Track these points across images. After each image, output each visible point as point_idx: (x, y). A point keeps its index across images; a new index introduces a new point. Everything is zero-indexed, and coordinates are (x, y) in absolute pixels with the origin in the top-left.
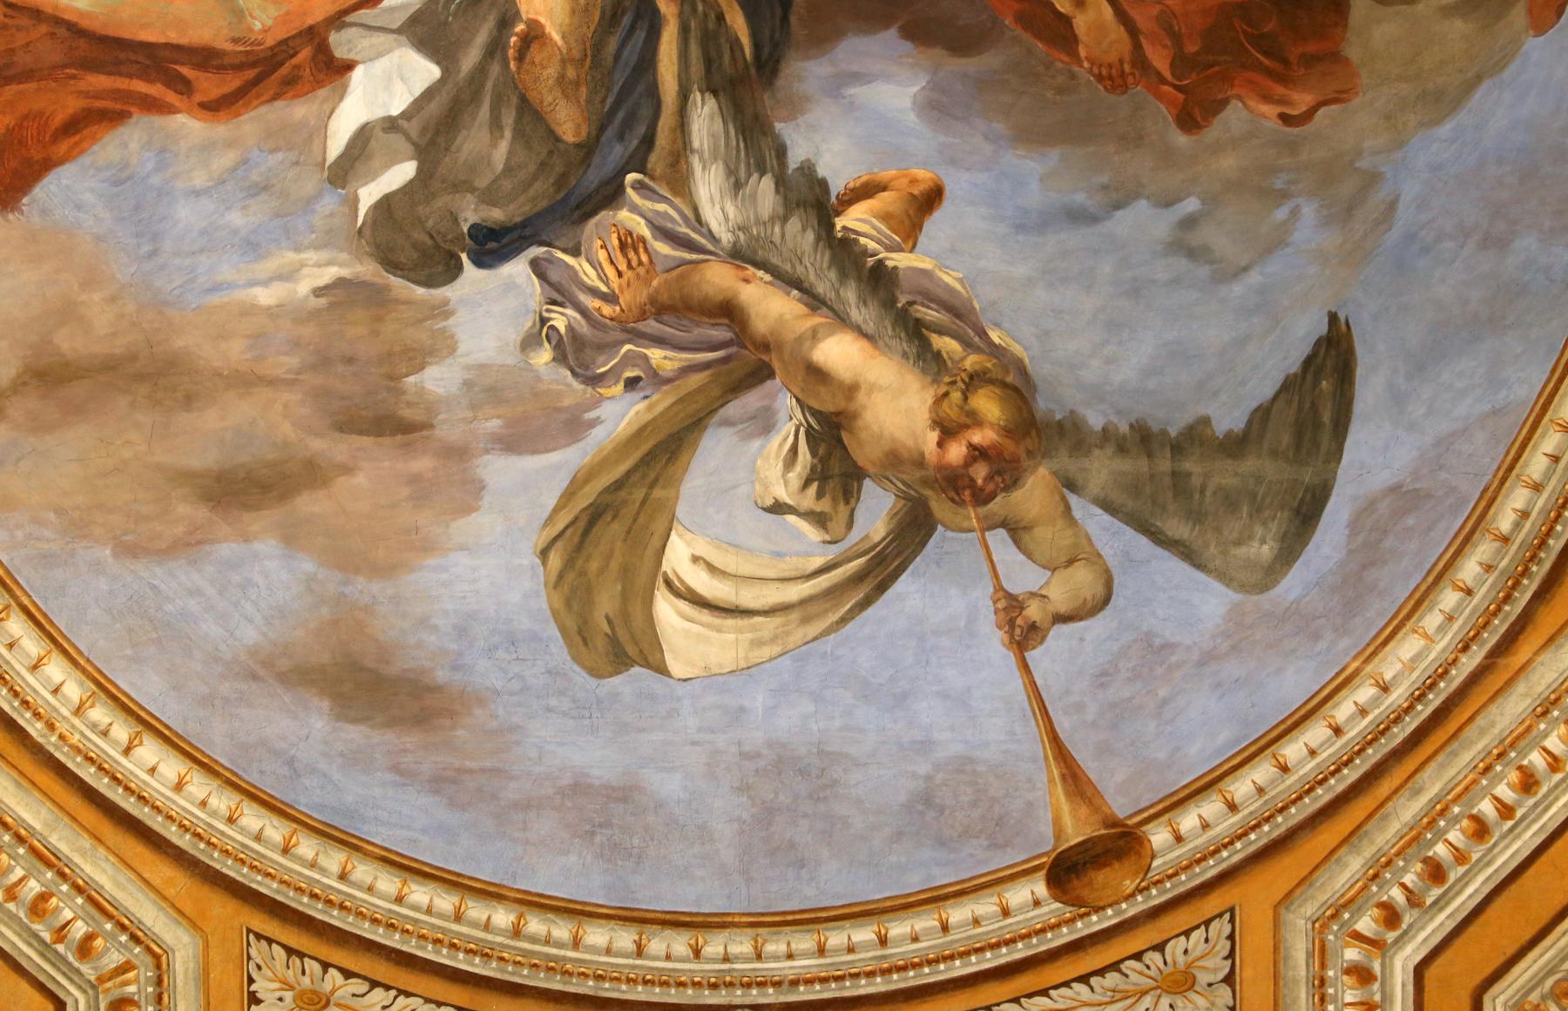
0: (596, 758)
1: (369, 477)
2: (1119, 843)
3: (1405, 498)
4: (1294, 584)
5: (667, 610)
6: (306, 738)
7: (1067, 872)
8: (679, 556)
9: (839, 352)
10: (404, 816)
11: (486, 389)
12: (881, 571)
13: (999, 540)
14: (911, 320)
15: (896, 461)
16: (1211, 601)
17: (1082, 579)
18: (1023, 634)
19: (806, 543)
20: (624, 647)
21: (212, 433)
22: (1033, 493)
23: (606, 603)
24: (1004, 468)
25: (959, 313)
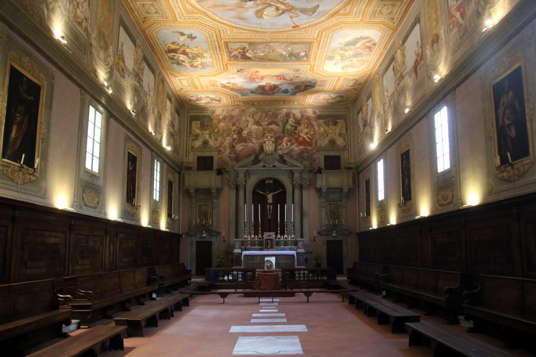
0: (259, 22)
1: (240, 9)
2: (298, 26)
3: (322, 11)
4: (313, 16)
5: (264, 16)
6: (237, 20)
7: (293, 27)
8: (265, 13)
9: (278, 5)
10: (245, 24)
11: (249, 6)
12: (281, 14)
13: (290, 14)
14: (284, 4)
15: (282, 9)
16: (306, 16)
17: (296, 15)
18: (291, 17)
19: (275, 13)
20: (261, 17)
21: (228, 8)
22: (293, 11)
23: (259, 15)
24: (291, 10)
25: (288, 4)
